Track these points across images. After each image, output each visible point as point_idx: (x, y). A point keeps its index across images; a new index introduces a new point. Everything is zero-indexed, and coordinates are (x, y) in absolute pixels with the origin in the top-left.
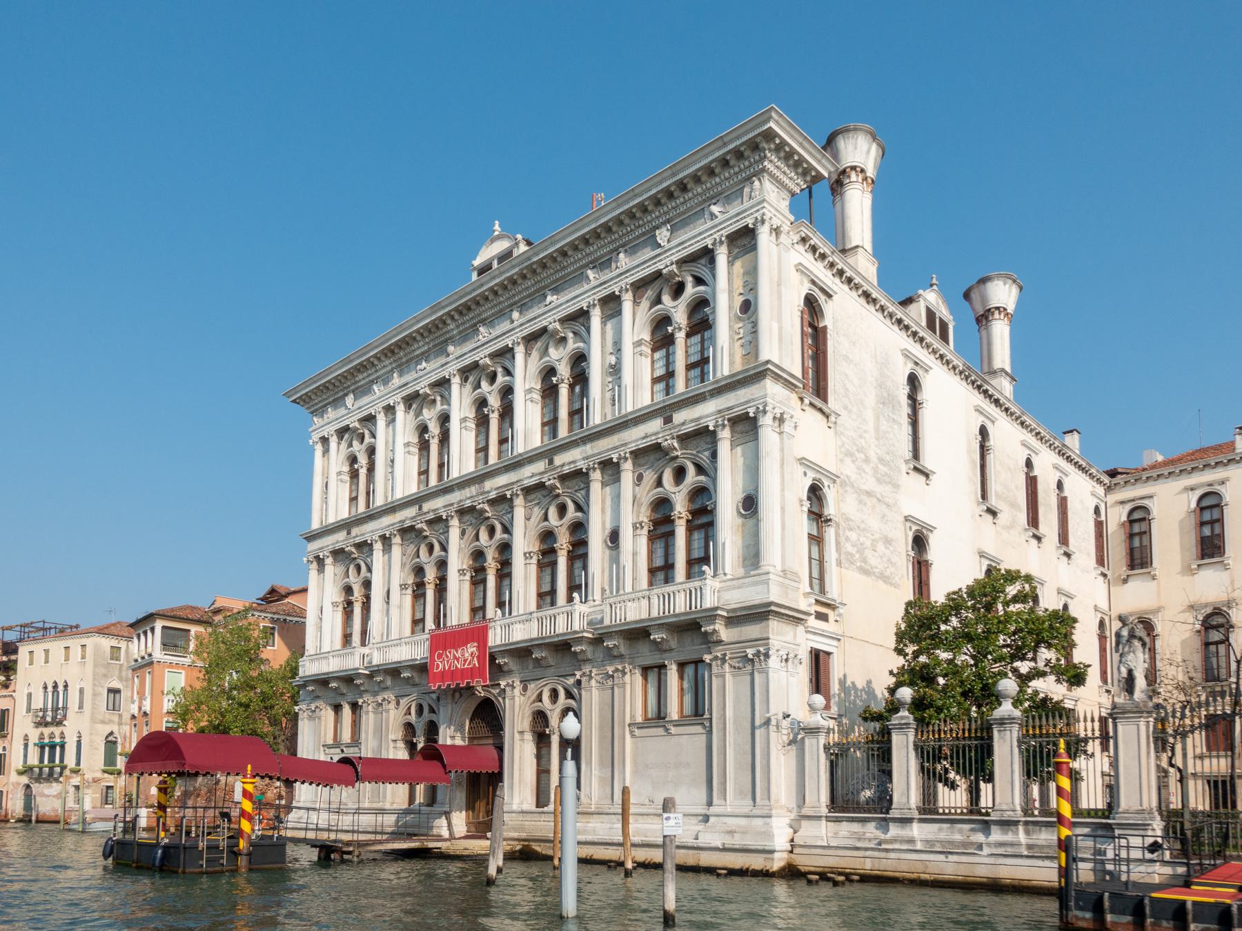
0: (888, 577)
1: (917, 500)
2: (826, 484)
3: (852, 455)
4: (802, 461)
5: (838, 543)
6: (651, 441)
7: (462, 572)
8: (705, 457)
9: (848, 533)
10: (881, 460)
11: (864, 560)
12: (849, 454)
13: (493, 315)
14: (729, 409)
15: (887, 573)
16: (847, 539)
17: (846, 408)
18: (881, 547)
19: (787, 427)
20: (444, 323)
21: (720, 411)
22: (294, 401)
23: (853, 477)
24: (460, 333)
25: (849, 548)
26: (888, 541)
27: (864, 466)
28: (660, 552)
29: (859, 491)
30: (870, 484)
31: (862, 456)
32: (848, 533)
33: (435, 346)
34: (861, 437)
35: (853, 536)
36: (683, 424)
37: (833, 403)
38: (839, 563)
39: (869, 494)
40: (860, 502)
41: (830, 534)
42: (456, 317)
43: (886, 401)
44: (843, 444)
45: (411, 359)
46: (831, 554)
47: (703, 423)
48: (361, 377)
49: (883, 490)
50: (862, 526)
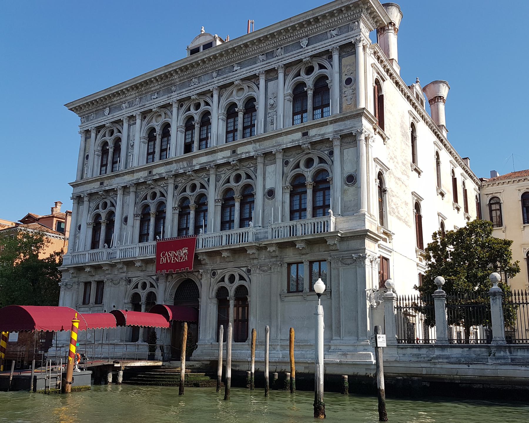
4: (376, 160)
6: (296, 144)
7: (174, 209)
8: (325, 155)
9: (392, 198)
13: (201, 73)
14: (341, 130)
20: (172, 75)
22: (71, 109)
24: (180, 81)
28: (297, 202)
29: (395, 177)
33: (164, 86)
36: (314, 136)
37: (387, 131)
40: (396, 183)
42: (179, 72)
45: (148, 92)
47: (327, 136)
48: (115, 99)
49: (404, 178)
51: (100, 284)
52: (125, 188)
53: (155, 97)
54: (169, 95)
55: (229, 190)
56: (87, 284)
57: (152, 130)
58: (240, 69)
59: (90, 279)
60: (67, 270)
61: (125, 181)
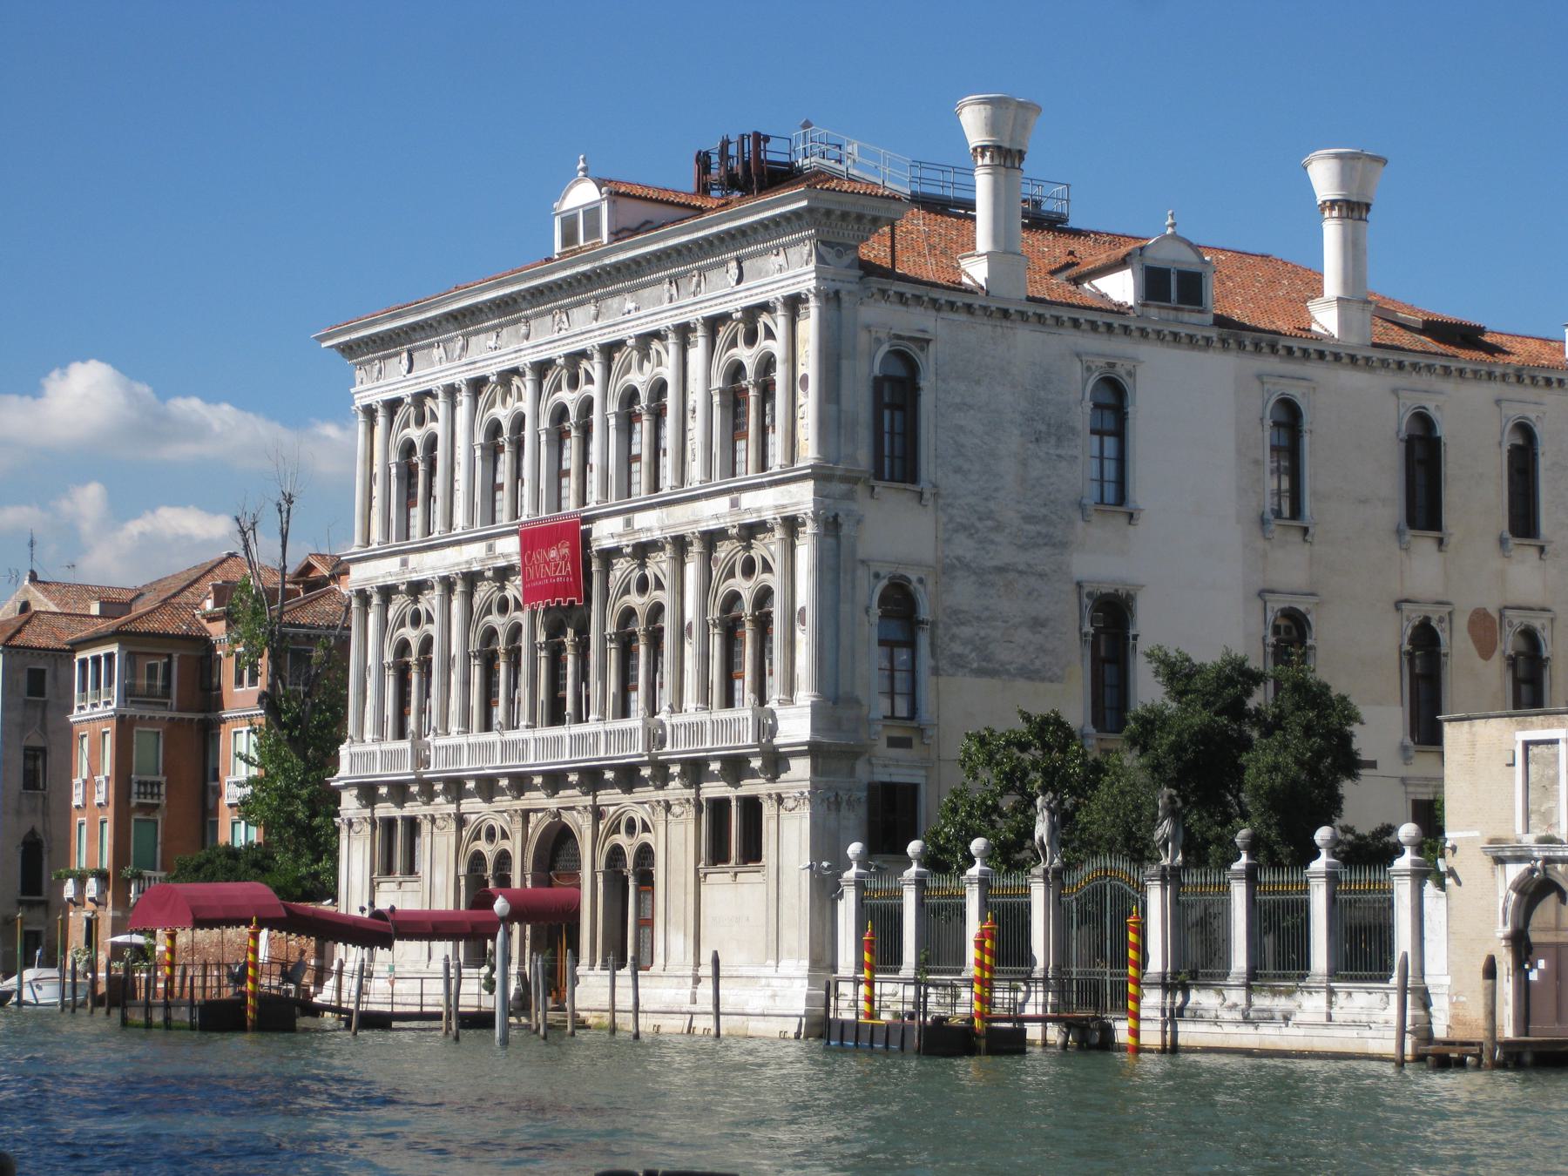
0: (1037, 671)
1: (1101, 559)
2: (914, 578)
3: (965, 528)
5: (933, 645)
9: (955, 630)
10: (1029, 519)
11: (987, 659)
12: (965, 528)
15: (1038, 663)
16: (953, 638)
17: (958, 470)
18: (1023, 635)
19: (845, 530)
21: (776, 507)
23: (969, 556)
25: (957, 648)
26: (1037, 624)
27: (992, 536)
30: (1005, 554)
31: (990, 523)
32: (955, 630)
34: (986, 499)
35: (966, 631)
38: (936, 671)
39: (1001, 570)
41: (923, 640)
43: (1046, 430)
44: (951, 519)
46: (925, 660)
50: (987, 614)
51: (412, 825)
52: (448, 584)
53: (492, 344)
54: (516, 347)
55: (629, 614)
56: (390, 823)
57: (495, 429)
58: (637, 309)
59: (396, 812)
60: (347, 786)
61: (447, 562)
